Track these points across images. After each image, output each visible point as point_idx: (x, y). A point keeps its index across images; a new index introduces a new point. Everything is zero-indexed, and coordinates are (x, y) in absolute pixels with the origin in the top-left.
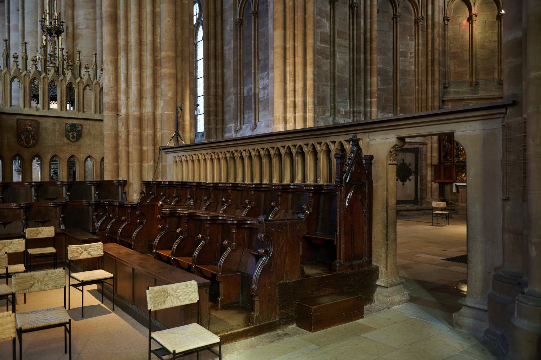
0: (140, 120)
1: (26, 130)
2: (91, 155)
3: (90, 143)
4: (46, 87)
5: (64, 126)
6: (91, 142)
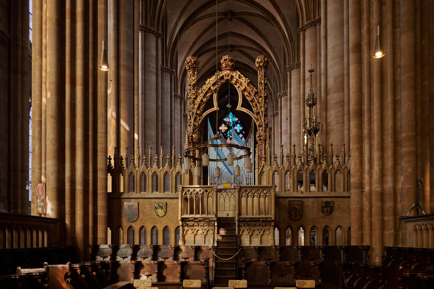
0: (382, 195)
1: (295, 208)
4: (308, 175)
5: (321, 203)
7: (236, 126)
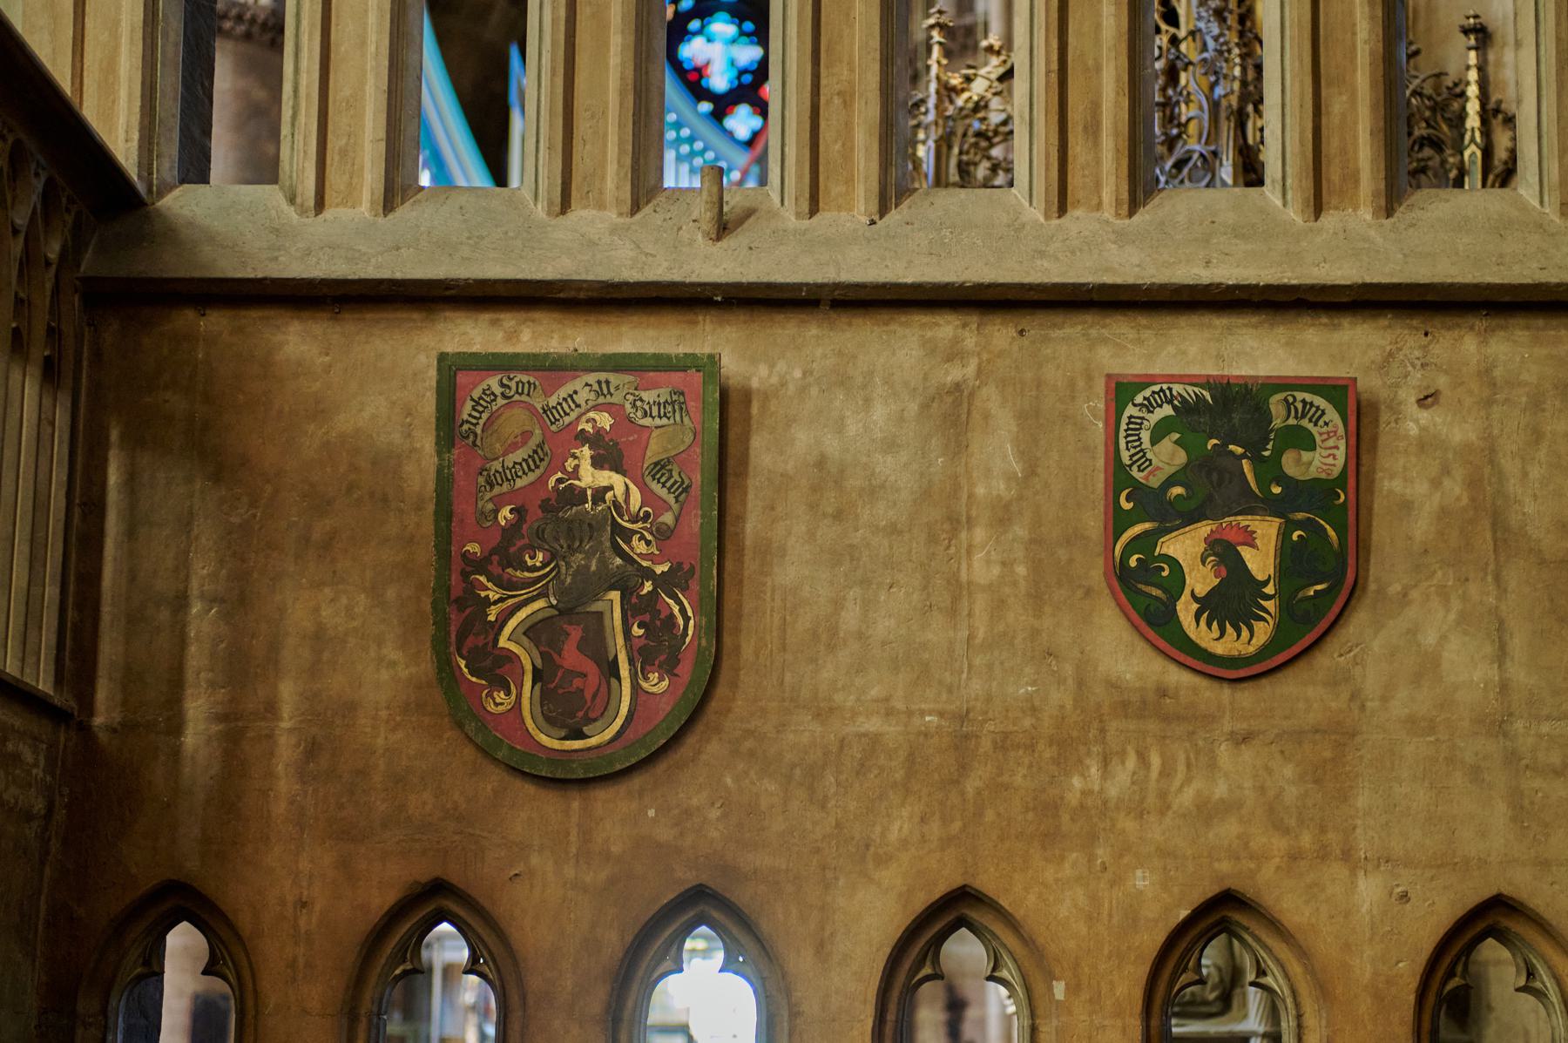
2: (1522, 884)
3: (1504, 687)
6: (1519, 674)
7: (700, 32)
